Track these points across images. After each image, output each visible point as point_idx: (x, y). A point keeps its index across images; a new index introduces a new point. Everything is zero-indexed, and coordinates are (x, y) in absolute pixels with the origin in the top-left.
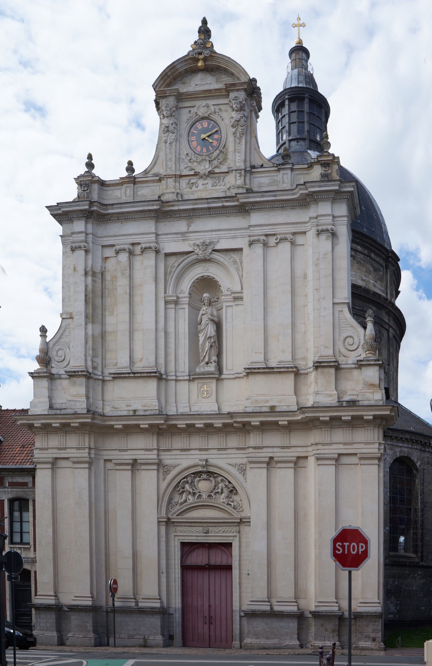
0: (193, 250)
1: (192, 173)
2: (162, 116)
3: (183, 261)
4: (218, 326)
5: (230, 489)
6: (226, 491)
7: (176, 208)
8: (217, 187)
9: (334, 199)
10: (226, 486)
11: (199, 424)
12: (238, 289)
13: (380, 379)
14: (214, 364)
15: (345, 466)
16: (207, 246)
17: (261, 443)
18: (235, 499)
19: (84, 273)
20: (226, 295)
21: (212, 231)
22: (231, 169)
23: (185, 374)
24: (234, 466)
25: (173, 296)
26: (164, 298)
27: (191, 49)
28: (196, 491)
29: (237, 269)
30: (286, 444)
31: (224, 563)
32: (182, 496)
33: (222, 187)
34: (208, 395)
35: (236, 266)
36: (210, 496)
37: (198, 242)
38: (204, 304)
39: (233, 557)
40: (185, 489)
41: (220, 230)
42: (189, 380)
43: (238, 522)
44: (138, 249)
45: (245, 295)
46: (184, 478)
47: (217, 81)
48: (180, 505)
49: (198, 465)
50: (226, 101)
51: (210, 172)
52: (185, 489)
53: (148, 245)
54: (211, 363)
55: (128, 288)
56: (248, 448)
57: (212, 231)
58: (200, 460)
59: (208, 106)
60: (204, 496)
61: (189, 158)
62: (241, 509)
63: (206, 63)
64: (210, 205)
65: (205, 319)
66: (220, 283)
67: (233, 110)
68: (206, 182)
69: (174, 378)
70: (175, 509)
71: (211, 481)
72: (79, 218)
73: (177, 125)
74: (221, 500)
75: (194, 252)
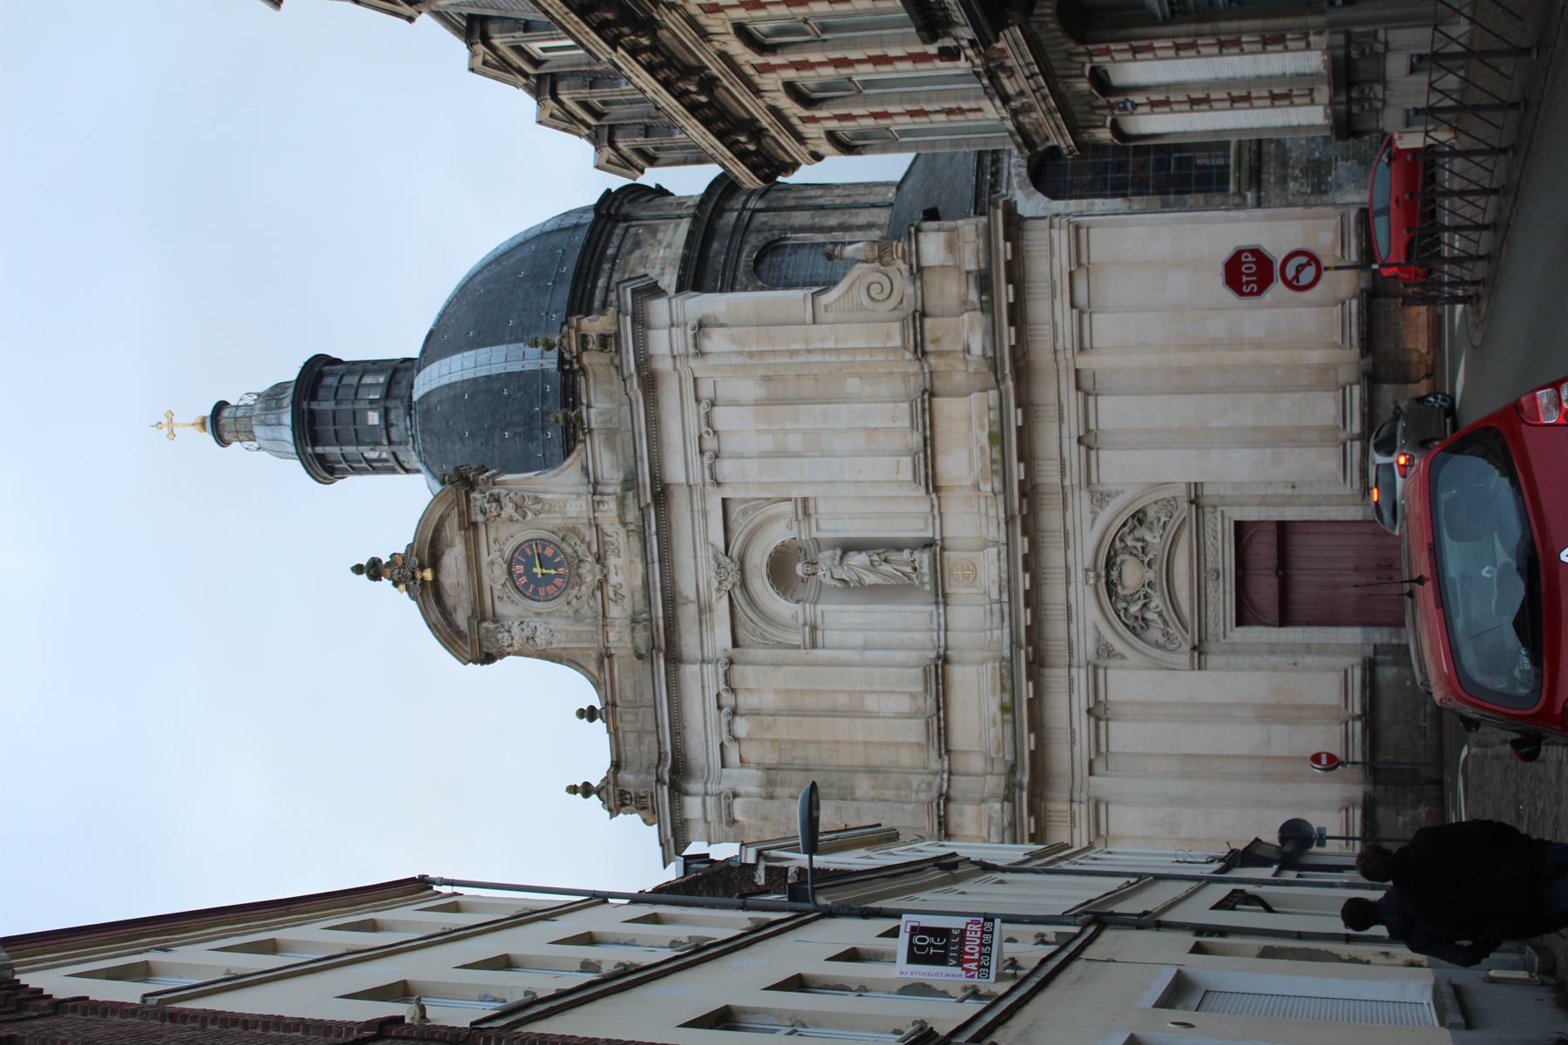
1: (599, 594)
2: (510, 649)
3: (743, 610)
4: (848, 547)
5: (1136, 523)
6: (1142, 532)
7: (661, 623)
8: (622, 547)
9: (643, 325)
10: (1131, 531)
11: (1024, 582)
12: (788, 507)
13: (938, 230)
14: (917, 555)
15: (1091, 296)
17: (1055, 462)
18: (1155, 515)
19: (770, 801)
20: (800, 531)
21: (695, 557)
22: (592, 521)
23: (935, 613)
24: (1095, 515)
25: (804, 631)
27: (406, 593)
28: (1142, 593)
29: (755, 508)
30: (1052, 412)
31: (1273, 539)
32: (1152, 620)
33: (620, 539)
34: (972, 568)
35: (750, 512)
36: (1149, 565)
37: (715, 584)
38: (814, 574)
39: (1262, 519)
40: (1139, 614)
41: (694, 541)
42: (946, 604)
43: (1197, 507)
44: (728, 699)
45: (797, 493)
46: (1119, 616)
47: (451, 546)
48: (1168, 626)
49: (1096, 586)
50: (482, 529)
51: (598, 560)
52: (1139, 614)
53: (722, 679)
54: (913, 562)
55: (792, 719)
56: (1063, 487)
57: (695, 557)
58: (1087, 583)
59: (492, 563)
60: (1150, 575)
61: (575, 600)
62: (1172, 502)
63: (426, 563)
64: (656, 559)
65: (840, 573)
66: (778, 542)
67: (499, 515)
68: (612, 568)
69: (942, 633)
70: (1177, 634)
71: (1123, 562)
72: (681, 808)
73: (522, 623)
74: (1157, 540)
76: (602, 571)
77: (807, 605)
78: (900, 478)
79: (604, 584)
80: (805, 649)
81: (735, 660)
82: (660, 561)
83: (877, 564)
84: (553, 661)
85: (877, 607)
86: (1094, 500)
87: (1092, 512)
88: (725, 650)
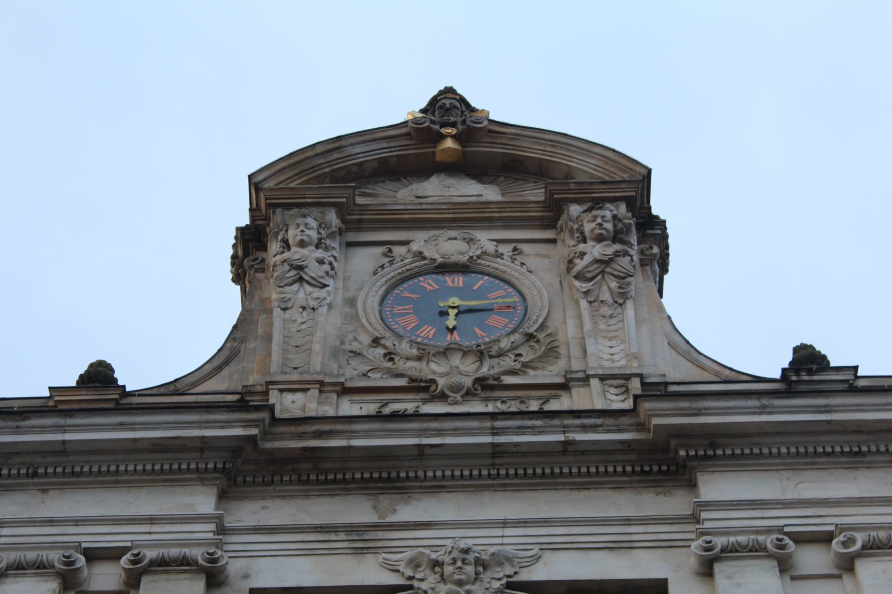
0: (409, 583)
16: (481, 569)
75: (411, 587)
76: (456, 389)
79: (422, 396)
82: (497, 451)
84: (235, 327)
88: (246, 576)
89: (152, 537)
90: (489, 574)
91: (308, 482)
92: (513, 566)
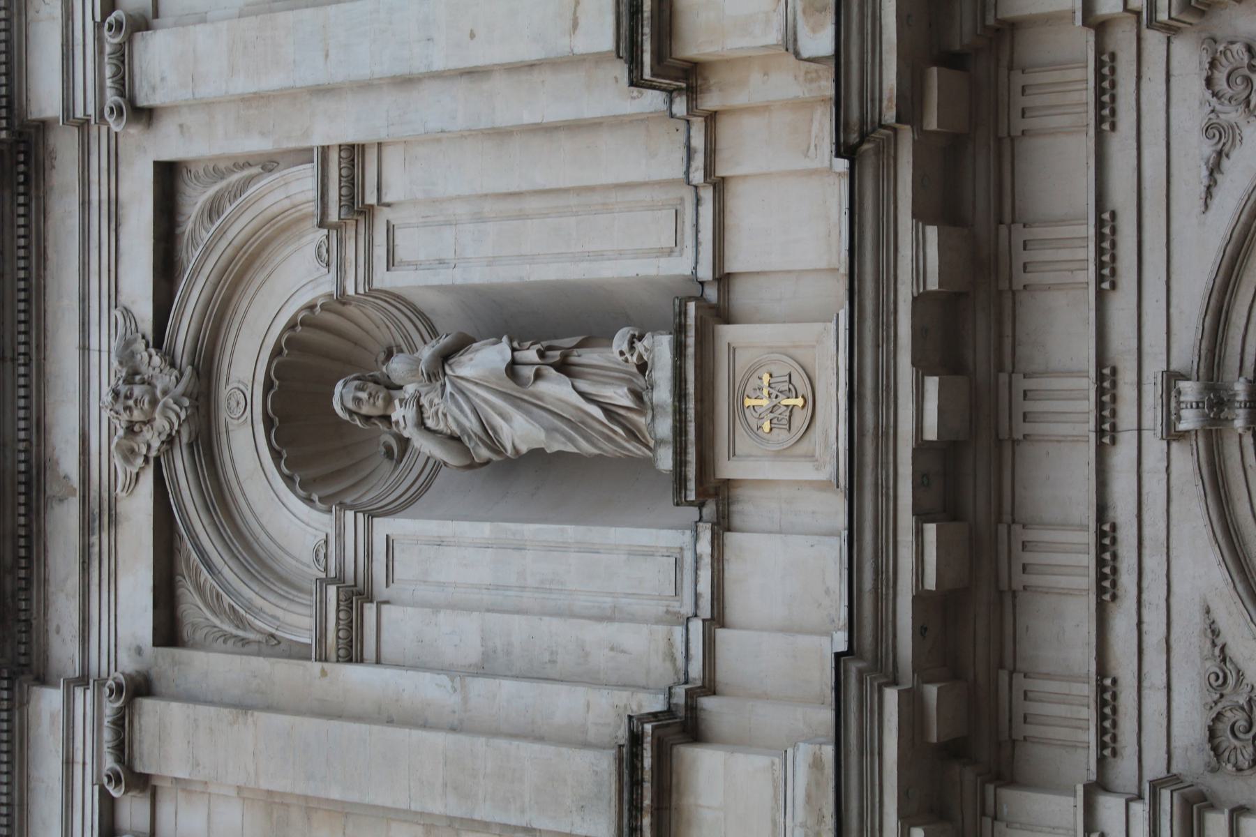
16: (138, 378)
25: (323, 602)
26: (326, 665)
75: (157, 459)
77: (350, 515)
78: (582, 45)
80: (323, 658)
81: (159, 686)
83: (529, 372)
85: (530, 530)
86: (1220, 77)
87: (1212, 129)
88: (139, 651)
89: (89, 760)
90: (144, 368)
91: (28, 580)
92: (135, 340)
